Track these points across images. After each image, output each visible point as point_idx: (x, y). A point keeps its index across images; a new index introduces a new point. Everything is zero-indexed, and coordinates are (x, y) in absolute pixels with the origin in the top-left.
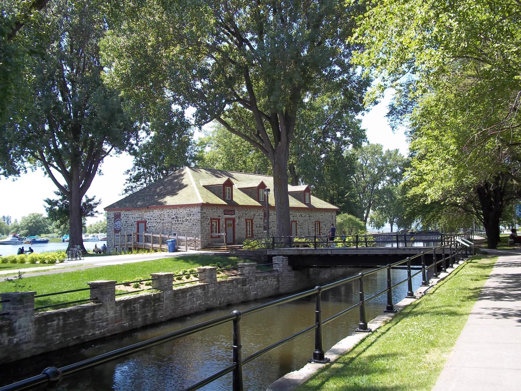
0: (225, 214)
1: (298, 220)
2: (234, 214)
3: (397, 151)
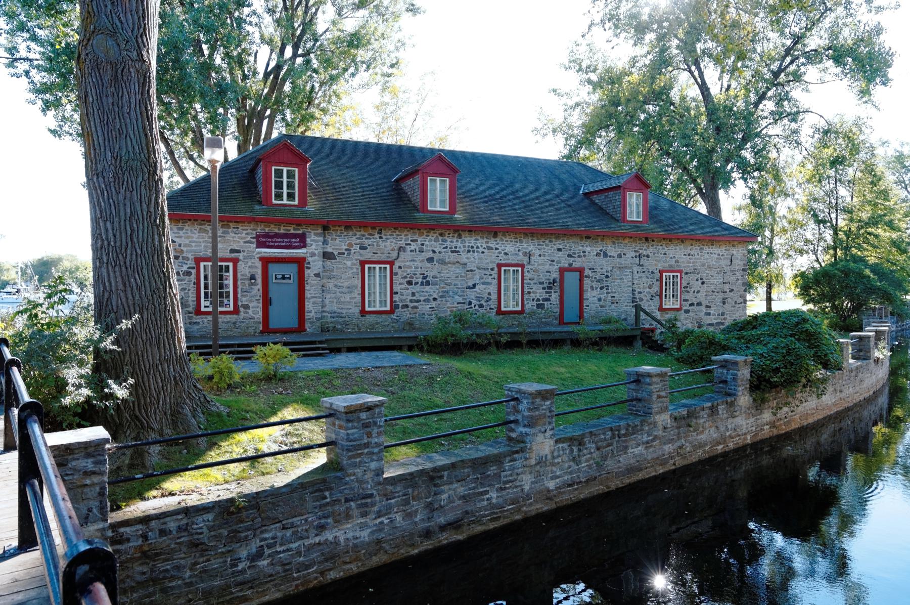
0: (260, 245)
1: (586, 265)
2: (305, 246)
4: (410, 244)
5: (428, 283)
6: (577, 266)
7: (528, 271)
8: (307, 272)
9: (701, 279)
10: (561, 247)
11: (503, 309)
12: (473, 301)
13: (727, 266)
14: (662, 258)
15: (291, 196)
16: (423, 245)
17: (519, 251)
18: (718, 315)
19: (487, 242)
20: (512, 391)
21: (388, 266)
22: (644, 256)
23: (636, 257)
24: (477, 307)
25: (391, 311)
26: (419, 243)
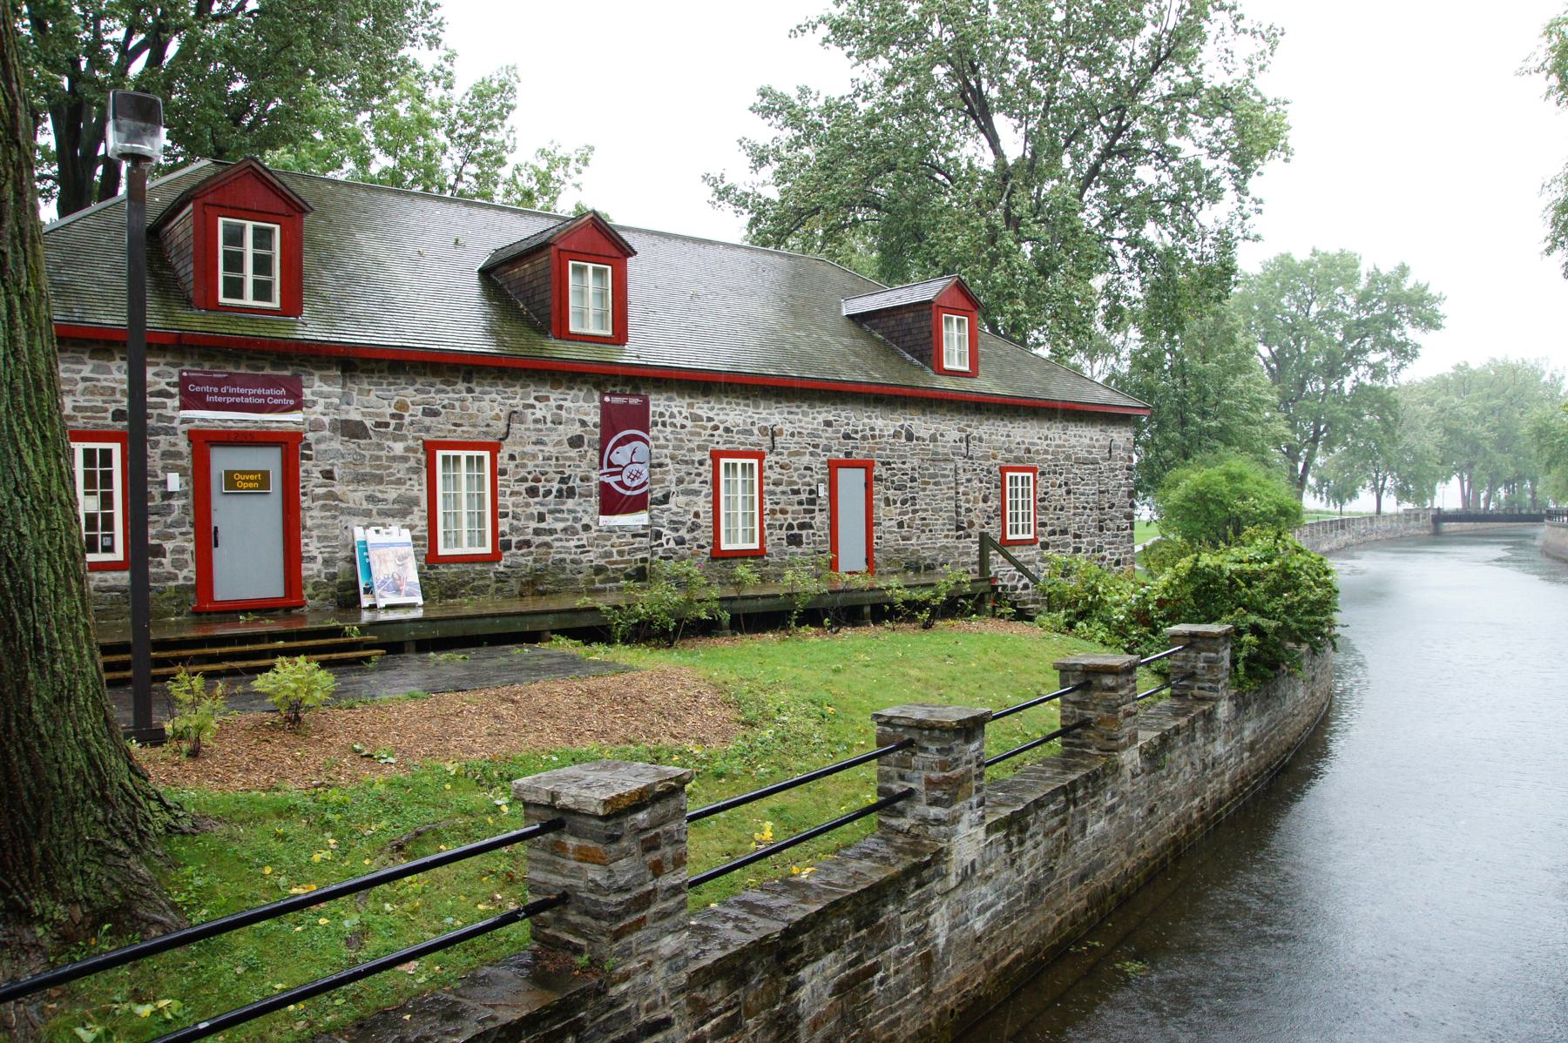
0: (192, 400)
2: (298, 406)
3: (1403, 271)
4: (533, 407)
5: (571, 493)
6: (860, 458)
7: (771, 467)
8: (305, 465)
9: (1066, 484)
10: (831, 418)
11: (724, 546)
12: (665, 531)
13: (1104, 459)
14: (1004, 442)
15: (262, 291)
16: (560, 407)
17: (753, 424)
18: (1094, 551)
19: (691, 405)
20: (894, 726)
21: (486, 454)
22: (974, 438)
23: (961, 441)
24: (672, 544)
25: (494, 558)
26: (553, 403)
